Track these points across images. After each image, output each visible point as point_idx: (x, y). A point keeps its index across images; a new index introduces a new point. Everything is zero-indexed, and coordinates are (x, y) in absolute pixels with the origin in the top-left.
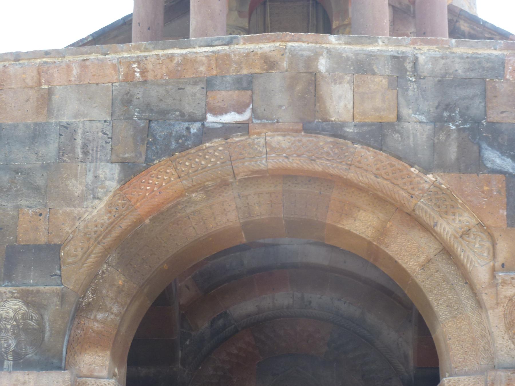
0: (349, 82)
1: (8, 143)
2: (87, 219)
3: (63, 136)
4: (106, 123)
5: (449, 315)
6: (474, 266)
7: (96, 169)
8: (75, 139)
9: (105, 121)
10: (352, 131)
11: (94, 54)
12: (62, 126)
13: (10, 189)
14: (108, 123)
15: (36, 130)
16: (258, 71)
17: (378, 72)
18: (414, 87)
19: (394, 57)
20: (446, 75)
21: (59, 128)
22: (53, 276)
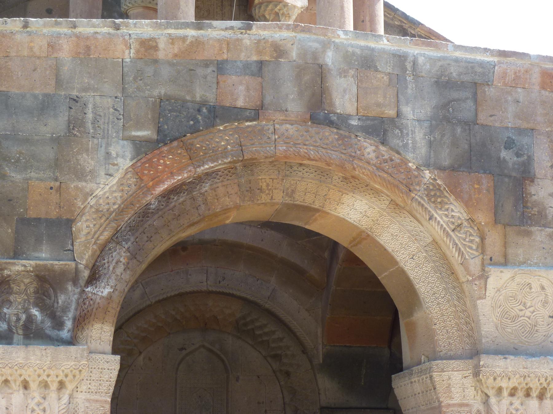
0: (353, 77)
1: (15, 113)
2: (98, 195)
3: (72, 109)
4: (117, 99)
5: (435, 302)
6: (465, 259)
7: (108, 145)
8: (85, 114)
9: (116, 97)
10: (357, 124)
11: (106, 28)
12: (72, 99)
13: (18, 161)
14: (119, 100)
15: (44, 101)
16: (267, 58)
17: (380, 69)
18: (412, 86)
19: (394, 55)
20: (441, 77)
21: (68, 100)
22: (66, 251)
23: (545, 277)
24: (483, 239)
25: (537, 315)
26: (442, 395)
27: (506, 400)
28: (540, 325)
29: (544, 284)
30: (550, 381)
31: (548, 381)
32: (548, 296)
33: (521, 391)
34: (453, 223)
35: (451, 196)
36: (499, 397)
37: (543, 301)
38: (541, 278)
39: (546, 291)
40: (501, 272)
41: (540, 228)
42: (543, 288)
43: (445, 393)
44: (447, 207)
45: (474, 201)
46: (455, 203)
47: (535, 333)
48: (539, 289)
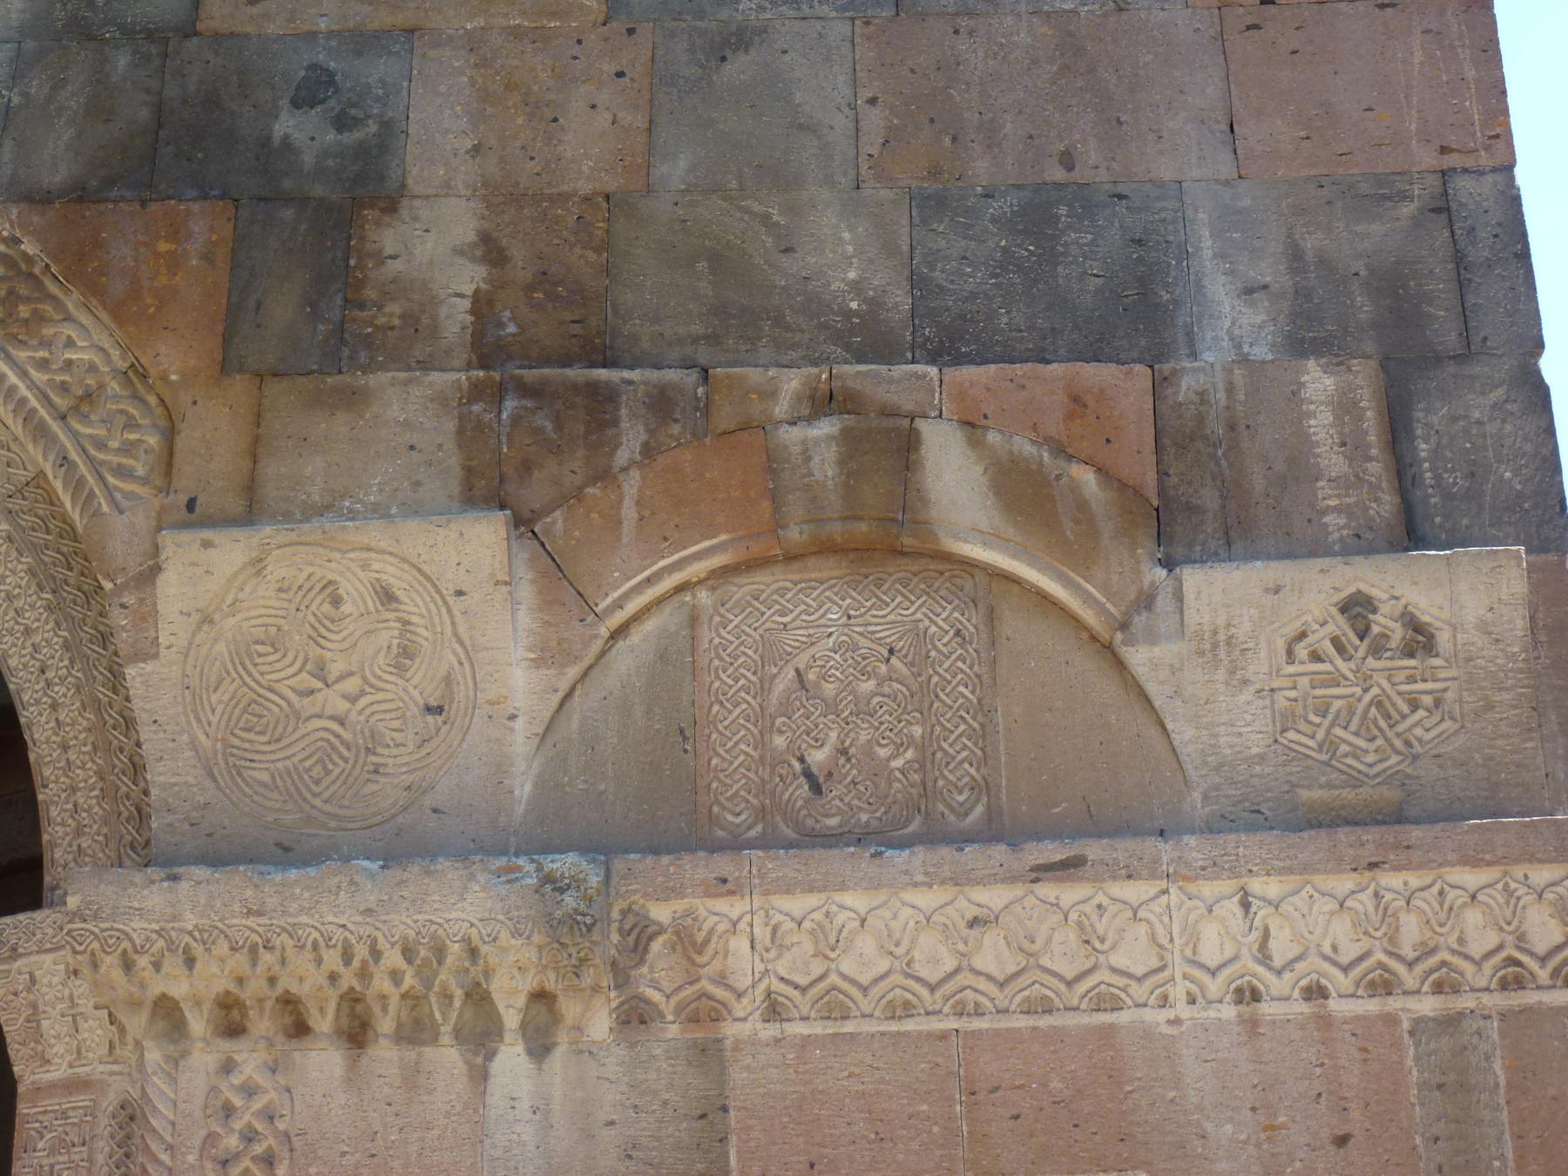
23: (391, 554)
24: (170, 433)
25: (375, 707)
26: (18, 1051)
27: (203, 1058)
28: (388, 746)
29: (392, 580)
30: (364, 962)
31: (356, 963)
32: (412, 628)
33: (262, 1010)
34: (64, 388)
35: (67, 291)
36: (175, 1042)
37: (395, 650)
38: (374, 555)
39: (403, 607)
40: (207, 545)
41: (403, 375)
42: (387, 597)
43: (23, 1044)
44: (48, 331)
45: (149, 301)
46: (85, 319)
47: (368, 780)
48: (370, 603)
